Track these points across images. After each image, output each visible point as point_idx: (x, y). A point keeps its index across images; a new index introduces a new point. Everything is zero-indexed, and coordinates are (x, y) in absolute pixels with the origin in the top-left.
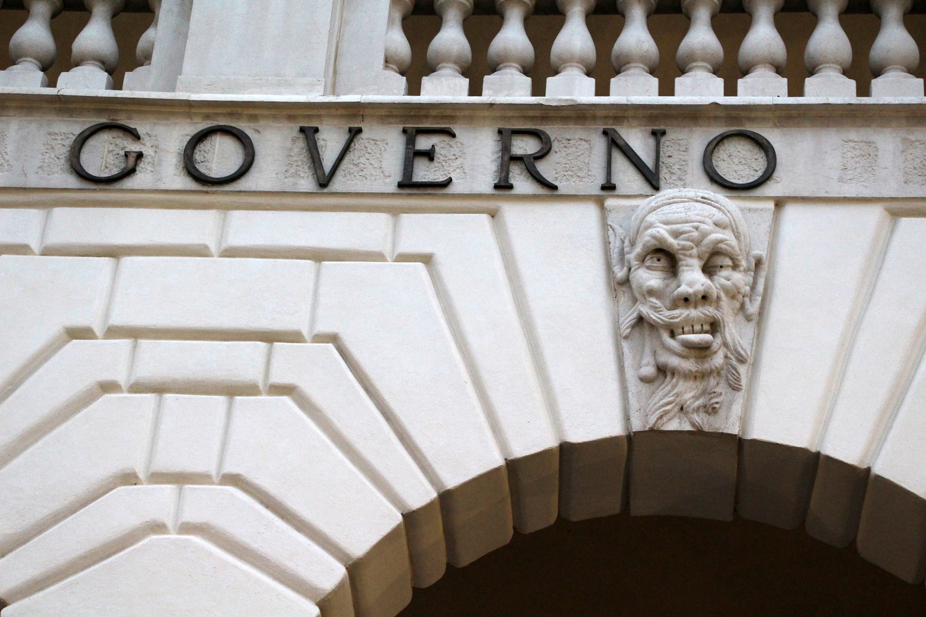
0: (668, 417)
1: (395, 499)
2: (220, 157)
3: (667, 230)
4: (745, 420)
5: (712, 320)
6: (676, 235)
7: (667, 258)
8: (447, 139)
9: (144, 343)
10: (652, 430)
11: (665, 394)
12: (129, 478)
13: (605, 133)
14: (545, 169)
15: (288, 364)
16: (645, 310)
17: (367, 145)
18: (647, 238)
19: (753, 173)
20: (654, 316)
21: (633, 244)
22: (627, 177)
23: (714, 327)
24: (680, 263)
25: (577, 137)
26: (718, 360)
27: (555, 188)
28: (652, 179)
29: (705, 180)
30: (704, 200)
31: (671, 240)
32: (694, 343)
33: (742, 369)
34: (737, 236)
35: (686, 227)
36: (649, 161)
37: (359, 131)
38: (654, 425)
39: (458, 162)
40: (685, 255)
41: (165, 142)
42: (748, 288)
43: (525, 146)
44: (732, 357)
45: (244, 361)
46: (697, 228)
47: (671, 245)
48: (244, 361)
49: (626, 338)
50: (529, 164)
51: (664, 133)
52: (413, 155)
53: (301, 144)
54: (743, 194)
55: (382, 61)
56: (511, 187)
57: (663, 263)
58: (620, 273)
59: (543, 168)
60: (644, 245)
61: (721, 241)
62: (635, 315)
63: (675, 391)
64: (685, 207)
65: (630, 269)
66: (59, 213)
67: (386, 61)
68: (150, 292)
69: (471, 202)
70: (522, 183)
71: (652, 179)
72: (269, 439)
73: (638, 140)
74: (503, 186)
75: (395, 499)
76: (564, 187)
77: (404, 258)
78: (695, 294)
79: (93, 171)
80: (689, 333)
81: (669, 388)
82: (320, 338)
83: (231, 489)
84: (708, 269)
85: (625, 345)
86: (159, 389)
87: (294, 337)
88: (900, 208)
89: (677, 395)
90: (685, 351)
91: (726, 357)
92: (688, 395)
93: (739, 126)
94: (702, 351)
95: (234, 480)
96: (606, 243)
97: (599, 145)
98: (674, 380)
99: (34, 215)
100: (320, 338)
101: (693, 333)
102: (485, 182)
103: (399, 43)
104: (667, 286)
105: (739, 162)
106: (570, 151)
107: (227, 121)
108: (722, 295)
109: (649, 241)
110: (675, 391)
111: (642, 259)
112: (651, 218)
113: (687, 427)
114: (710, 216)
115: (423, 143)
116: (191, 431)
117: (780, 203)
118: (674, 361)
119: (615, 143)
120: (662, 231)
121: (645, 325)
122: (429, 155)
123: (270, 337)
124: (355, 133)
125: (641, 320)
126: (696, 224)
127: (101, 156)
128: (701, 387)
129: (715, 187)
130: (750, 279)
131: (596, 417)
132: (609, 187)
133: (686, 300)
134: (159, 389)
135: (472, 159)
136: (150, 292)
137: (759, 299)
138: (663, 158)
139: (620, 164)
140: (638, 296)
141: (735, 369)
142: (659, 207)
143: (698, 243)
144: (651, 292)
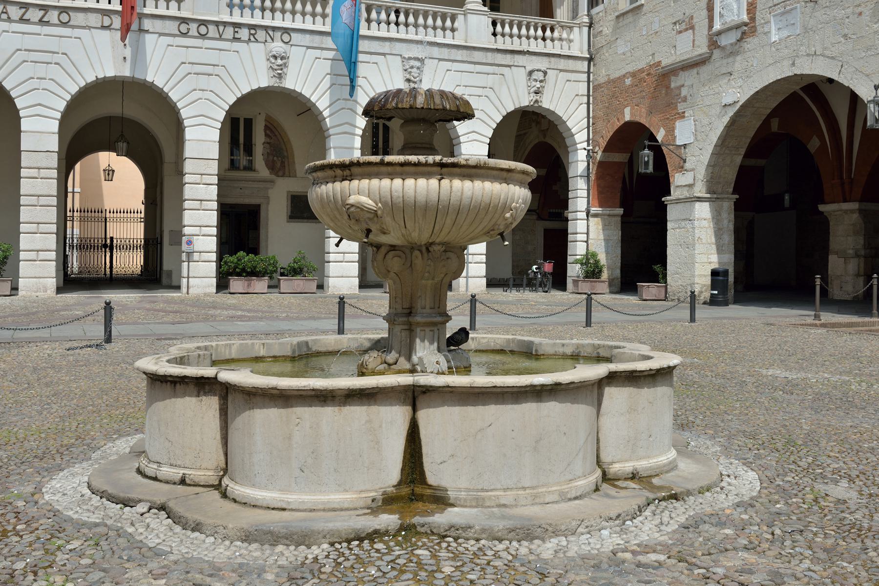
7: (275, 57)
22: (269, 39)
43: (253, 32)
45: (209, 69)
48: (209, 69)
50: (253, 35)
64: (277, 46)
68: (194, 55)
69: (244, 41)
70: (252, 39)
71: (273, 40)
93: (286, 30)
94: (280, 74)
105: (286, 37)
107: (204, 23)
135: (244, 33)
136: (194, 55)
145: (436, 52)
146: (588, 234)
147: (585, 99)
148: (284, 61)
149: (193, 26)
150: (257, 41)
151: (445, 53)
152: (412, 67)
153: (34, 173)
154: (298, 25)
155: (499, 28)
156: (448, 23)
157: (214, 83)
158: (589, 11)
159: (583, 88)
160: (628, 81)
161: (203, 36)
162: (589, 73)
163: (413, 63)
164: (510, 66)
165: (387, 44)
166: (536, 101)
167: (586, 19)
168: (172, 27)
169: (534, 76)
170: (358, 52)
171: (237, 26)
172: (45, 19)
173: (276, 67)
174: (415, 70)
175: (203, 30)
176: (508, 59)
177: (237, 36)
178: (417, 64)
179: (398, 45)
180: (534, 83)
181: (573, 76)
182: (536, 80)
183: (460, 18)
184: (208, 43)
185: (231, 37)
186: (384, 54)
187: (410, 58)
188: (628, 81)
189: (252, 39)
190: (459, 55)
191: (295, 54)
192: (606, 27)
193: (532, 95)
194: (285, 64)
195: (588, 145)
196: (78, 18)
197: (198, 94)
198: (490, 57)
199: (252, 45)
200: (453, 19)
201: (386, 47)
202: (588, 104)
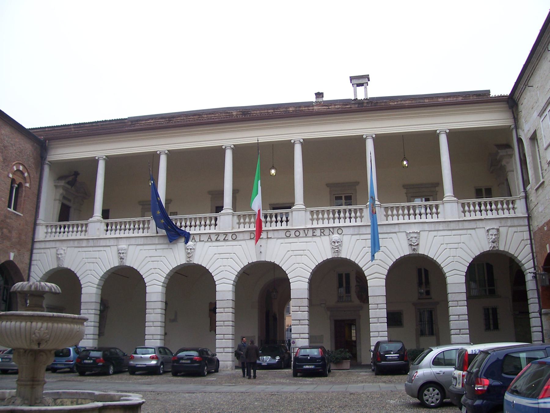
7: (334, 242)
11: (335, 254)
15: (306, 252)
22: (331, 233)
41: (293, 232)
43: (322, 231)
52: (313, 232)
64: (336, 237)
68: (294, 246)
69: (318, 236)
70: (322, 234)
72: (304, 259)
73: (331, 230)
88: (352, 235)
93: (340, 228)
105: (340, 232)
107: (297, 230)
127: (288, 234)
131: (330, 256)
135: (318, 232)
136: (294, 246)
145: (426, 227)
146: (542, 326)
147: (529, 242)
151: (432, 227)
152: (412, 238)
153: (222, 310)
154: (348, 223)
155: (466, 208)
156: (434, 210)
157: (304, 259)
158: (525, 188)
159: (526, 235)
160: (546, 228)
162: (529, 225)
163: (412, 235)
164: (474, 229)
165: (397, 226)
166: (494, 247)
167: (523, 194)
168: (282, 234)
169: (490, 233)
170: (378, 234)
171: (314, 229)
172: (226, 239)
174: (414, 239)
175: (297, 234)
176: (473, 225)
177: (314, 234)
178: (416, 235)
179: (403, 226)
180: (491, 237)
181: (519, 229)
182: (492, 235)
183: (441, 207)
186: (395, 233)
187: (410, 233)
188: (546, 228)
190: (441, 227)
191: (346, 239)
192: (532, 197)
193: (491, 244)
195: (535, 269)
196: (240, 236)
197: (297, 265)
198: (460, 225)
200: (437, 207)
201: (396, 229)
202: (531, 244)
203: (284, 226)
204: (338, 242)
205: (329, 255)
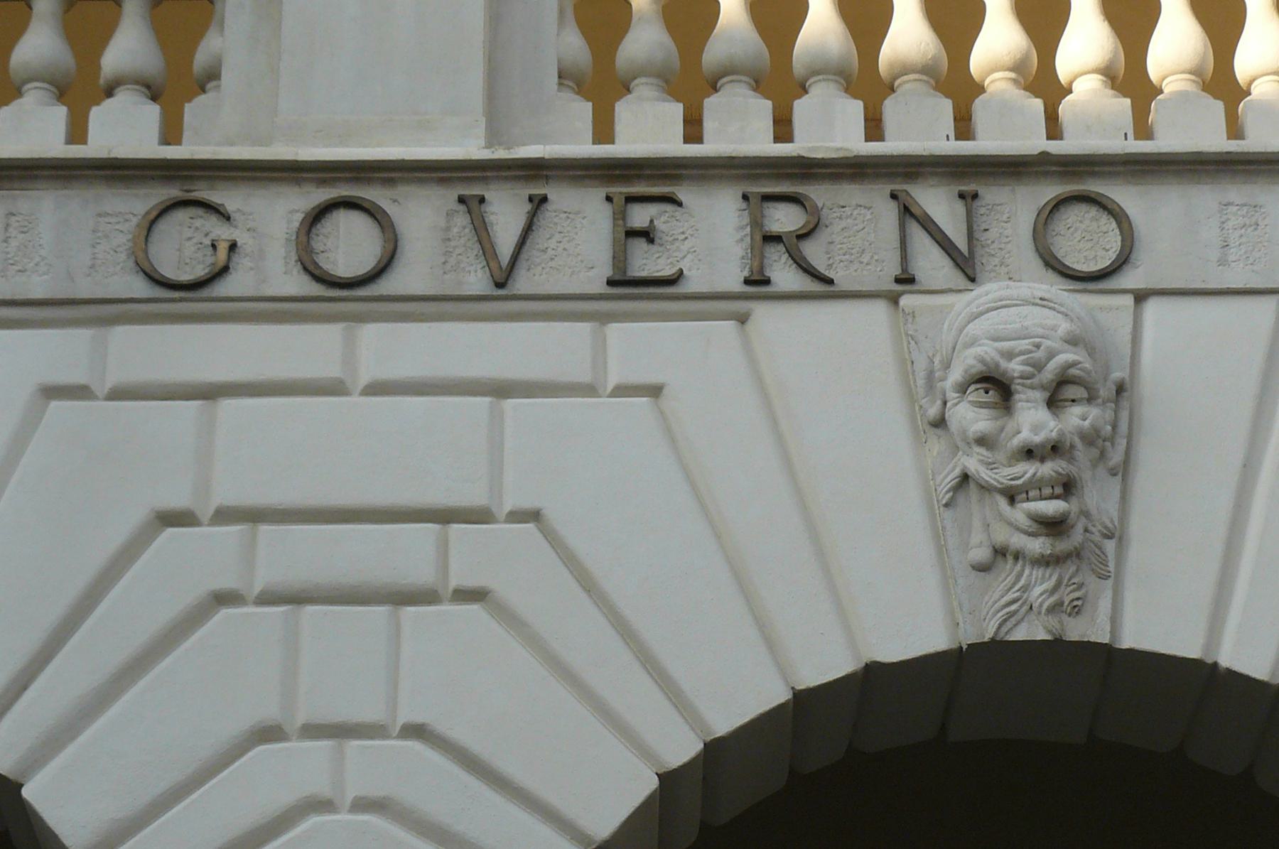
0: (1013, 620)
1: (644, 751)
2: (349, 245)
3: (996, 349)
4: (1115, 620)
5: (1065, 480)
6: (1010, 355)
7: (996, 386)
8: (669, 208)
9: (265, 529)
10: (993, 640)
11: (1001, 586)
12: (269, 733)
13: (894, 196)
14: (813, 251)
16: (973, 462)
17: (556, 220)
18: (971, 361)
19: (1101, 253)
20: (986, 475)
21: (947, 366)
22: (931, 264)
23: (1068, 487)
24: (1017, 397)
25: (854, 203)
26: (1077, 537)
27: (830, 282)
28: (967, 266)
29: (1035, 263)
30: (1043, 302)
31: (1004, 364)
32: (1046, 517)
33: (1110, 546)
34: (1091, 352)
35: (1024, 344)
36: (959, 239)
37: (544, 199)
38: (996, 633)
39: (688, 244)
40: (1023, 385)
42: (1109, 428)
43: (784, 219)
44: (1094, 530)
45: (406, 553)
46: (1038, 346)
47: (1005, 373)
48: (406, 553)
49: (946, 505)
51: (975, 196)
53: (462, 220)
54: (1091, 286)
55: (556, 79)
56: (767, 282)
57: (992, 396)
58: (933, 411)
59: (813, 251)
60: (966, 371)
61: (1074, 364)
62: (957, 472)
63: (1022, 582)
64: (1012, 311)
65: (945, 403)
66: (121, 333)
67: (560, 77)
68: (264, 451)
69: (712, 302)
70: (784, 276)
71: (967, 266)
74: (758, 280)
75: (644, 751)
76: (843, 277)
77: (623, 391)
78: (1043, 445)
79: (170, 273)
80: (1035, 500)
81: (1011, 579)
82: (518, 516)
83: (414, 745)
84: (1053, 403)
85: (948, 514)
86: (297, 598)
87: (479, 516)
89: (1025, 589)
90: (1034, 527)
91: (1086, 530)
92: (1038, 590)
94: (1053, 526)
95: (416, 731)
96: (905, 366)
97: (889, 212)
98: (1018, 567)
99: (82, 336)
100: (518, 516)
101: (1041, 499)
102: (729, 273)
103: (574, 45)
104: (1002, 429)
105: (1087, 241)
106: (843, 224)
107: (349, 185)
108: (1077, 441)
109: (973, 366)
110: (1022, 582)
111: (963, 389)
112: (974, 328)
113: (1042, 635)
114: (1054, 328)
115: (640, 216)
116: (342, 660)
117: (1141, 297)
118: (1018, 541)
119: (907, 211)
120: (988, 350)
121: (972, 485)
122: (647, 234)
123: (445, 516)
124: (539, 202)
125: (965, 478)
126: (1037, 340)
128: (1054, 578)
129: (1051, 275)
130: (1109, 414)
131: (912, 621)
132: (906, 279)
133: (1029, 453)
134: (297, 598)
135: (708, 236)
137: (1124, 442)
138: (977, 235)
139: (921, 242)
140: (960, 444)
141: (1100, 548)
142: (982, 314)
143: (1039, 366)
144: (982, 441)
148: (1077, 417)
149: (270, 218)
150: (824, 286)
157: (448, 667)
161: (344, 293)
171: (640, 183)
173: (1006, 474)
177: (646, 262)
184: (387, 347)
185: (594, 278)
189: (785, 264)
191: (1186, 357)
194: (1091, 438)
199: (769, 319)
203: (124, 128)
204: (1056, 395)
205: (896, 594)
